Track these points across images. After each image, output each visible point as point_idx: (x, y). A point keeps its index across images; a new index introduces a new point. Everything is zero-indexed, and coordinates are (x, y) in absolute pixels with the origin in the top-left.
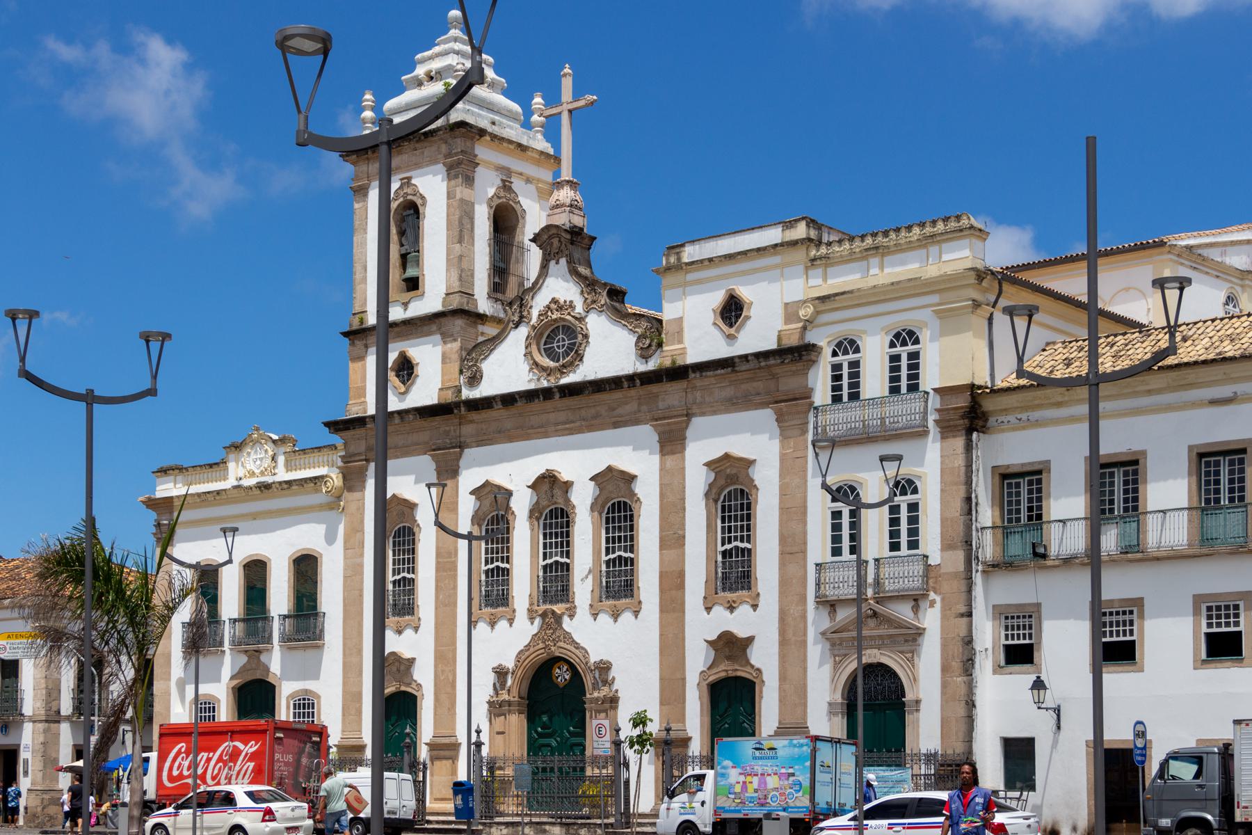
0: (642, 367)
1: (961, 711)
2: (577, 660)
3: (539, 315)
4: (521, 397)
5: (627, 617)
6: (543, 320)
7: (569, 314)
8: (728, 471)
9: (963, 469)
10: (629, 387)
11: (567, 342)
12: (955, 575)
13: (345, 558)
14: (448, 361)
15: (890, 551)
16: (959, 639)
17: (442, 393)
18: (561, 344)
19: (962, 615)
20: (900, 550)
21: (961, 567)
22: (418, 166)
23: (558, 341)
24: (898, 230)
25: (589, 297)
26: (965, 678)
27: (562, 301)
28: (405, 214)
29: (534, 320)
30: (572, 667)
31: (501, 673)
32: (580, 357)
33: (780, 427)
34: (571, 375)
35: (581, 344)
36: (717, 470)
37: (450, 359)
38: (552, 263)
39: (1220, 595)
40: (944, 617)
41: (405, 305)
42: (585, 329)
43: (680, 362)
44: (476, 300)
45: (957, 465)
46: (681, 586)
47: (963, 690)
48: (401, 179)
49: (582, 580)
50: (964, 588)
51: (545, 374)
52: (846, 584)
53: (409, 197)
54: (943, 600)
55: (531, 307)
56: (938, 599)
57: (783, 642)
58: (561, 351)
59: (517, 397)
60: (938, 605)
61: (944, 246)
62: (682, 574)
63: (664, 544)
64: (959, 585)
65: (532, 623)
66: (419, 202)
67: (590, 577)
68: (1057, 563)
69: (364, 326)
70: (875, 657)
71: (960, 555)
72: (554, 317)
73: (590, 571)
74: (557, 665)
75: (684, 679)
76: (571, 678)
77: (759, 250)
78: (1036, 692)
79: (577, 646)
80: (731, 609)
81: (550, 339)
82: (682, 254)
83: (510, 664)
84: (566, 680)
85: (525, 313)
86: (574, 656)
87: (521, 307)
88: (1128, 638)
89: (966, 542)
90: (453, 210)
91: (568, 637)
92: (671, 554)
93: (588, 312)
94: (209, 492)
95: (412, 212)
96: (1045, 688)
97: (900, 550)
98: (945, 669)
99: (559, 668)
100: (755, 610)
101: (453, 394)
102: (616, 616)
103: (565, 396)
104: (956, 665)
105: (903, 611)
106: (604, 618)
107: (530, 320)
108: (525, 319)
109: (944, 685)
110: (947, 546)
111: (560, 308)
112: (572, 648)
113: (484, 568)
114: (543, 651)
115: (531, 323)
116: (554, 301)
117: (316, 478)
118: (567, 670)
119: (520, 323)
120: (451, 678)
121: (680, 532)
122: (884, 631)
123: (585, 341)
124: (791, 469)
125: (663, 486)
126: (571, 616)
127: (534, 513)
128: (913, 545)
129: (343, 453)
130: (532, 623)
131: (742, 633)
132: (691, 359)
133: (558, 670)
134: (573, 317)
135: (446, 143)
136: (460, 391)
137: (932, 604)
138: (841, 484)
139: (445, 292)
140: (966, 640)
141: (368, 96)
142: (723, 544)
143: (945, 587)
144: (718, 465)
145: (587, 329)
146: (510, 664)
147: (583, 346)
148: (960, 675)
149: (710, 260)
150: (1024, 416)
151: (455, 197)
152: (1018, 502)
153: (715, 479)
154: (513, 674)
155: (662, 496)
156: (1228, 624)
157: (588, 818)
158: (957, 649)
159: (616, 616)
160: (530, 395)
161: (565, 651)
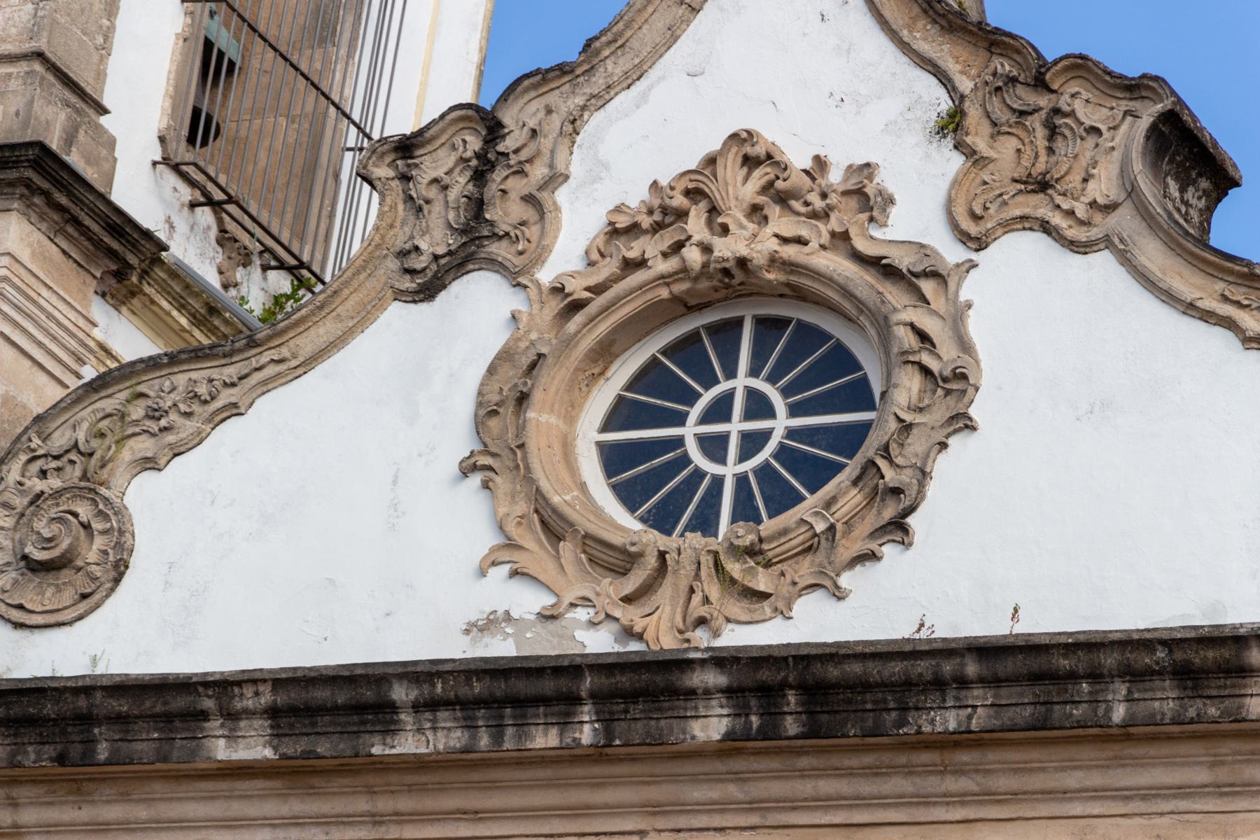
3: (614, 232)
6: (631, 265)
11: (781, 423)
18: (736, 427)
27: (799, 159)
35: (906, 428)
42: (948, 346)
44: (111, 143)
51: (611, 589)
55: (556, 179)
58: (730, 470)
59: (400, 693)
72: (726, 248)
85: (505, 213)
87: (480, 177)
93: (980, 243)
107: (540, 258)
108: (499, 250)
115: (546, 275)
119: (469, 258)
123: (938, 414)
145: (966, 346)
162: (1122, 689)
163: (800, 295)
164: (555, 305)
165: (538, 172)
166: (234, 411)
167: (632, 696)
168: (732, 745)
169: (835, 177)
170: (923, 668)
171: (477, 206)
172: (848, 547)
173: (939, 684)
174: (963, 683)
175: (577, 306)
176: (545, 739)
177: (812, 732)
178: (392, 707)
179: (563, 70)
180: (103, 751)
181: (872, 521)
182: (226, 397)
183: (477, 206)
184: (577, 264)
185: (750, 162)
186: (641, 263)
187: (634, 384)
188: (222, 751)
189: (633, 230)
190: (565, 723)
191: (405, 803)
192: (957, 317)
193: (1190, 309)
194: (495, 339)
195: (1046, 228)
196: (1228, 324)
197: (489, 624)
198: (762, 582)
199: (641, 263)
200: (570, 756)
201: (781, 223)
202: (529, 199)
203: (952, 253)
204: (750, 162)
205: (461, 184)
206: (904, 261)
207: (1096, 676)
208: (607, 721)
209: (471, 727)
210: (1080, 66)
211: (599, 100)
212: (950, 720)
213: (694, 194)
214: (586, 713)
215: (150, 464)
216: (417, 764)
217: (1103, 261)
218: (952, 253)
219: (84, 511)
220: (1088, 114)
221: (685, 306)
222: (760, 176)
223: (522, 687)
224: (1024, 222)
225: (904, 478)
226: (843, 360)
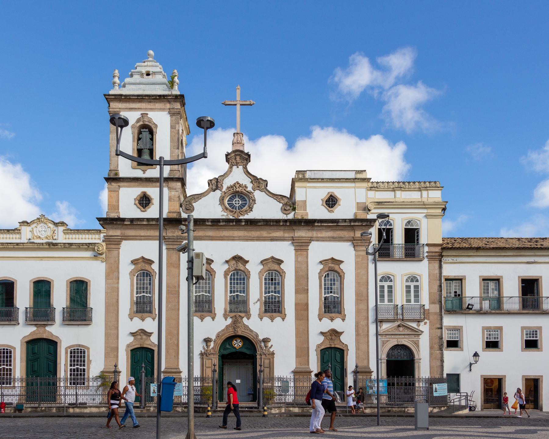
0: (284, 217)
1: (439, 363)
2: (252, 337)
4: (223, 221)
5: (278, 320)
7: (245, 190)
8: (330, 265)
9: (438, 275)
10: (283, 225)
11: (240, 202)
12: (435, 313)
13: (106, 283)
14: (172, 200)
15: (414, 302)
16: (438, 337)
17: (170, 214)
18: (237, 202)
19: (439, 328)
20: (411, 303)
21: (438, 311)
22: (152, 109)
23: (236, 201)
24: (414, 183)
25: (256, 184)
26: (440, 352)
27: (241, 183)
28: (142, 130)
29: (224, 189)
30: (243, 338)
31: (207, 341)
32: (251, 209)
33: (355, 250)
34: (246, 215)
36: (325, 264)
37: (174, 199)
38: (235, 167)
39: (531, 327)
40: (430, 329)
41: (144, 171)
43: (305, 218)
45: (435, 273)
46: (307, 309)
47: (439, 356)
48: (142, 114)
49: (254, 303)
50: (439, 318)
52: (390, 314)
53: (147, 123)
54: (430, 322)
56: (428, 321)
57: (358, 334)
60: (428, 324)
61: (430, 192)
62: (307, 305)
63: (297, 292)
64: (438, 317)
65: (226, 320)
66: (153, 126)
67: (259, 302)
68: (474, 312)
69: (117, 177)
70: (402, 342)
71: (437, 306)
73: (258, 300)
74: (235, 339)
75: (308, 348)
76: (244, 345)
77: (347, 179)
78: (475, 357)
79: (251, 331)
80: (332, 320)
81: (231, 200)
82: (306, 175)
83: (213, 337)
84: (240, 346)
85: (219, 186)
86: (250, 336)
88: (496, 340)
89: (440, 302)
90: (174, 134)
91: (246, 327)
92: (302, 296)
93: (255, 191)
94: (10, 243)
95: (147, 130)
96: (479, 356)
97: (411, 303)
98: (431, 348)
99: (236, 340)
100: (343, 321)
101: (177, 215)
102: (272, 319)
103: (247, 224)
104: (436, 346)
105: (414, 325)
106: (266, 320)
109: (431, 354)
110: (432, 302)
111: (240, 186)
112: (250, 333)
113: (194, 294)
114: (233, 332)
115: (223, 190)
116: (238, 183)
117: (89, 244)
118: (240, 341)
120: (176, 343)
121: (306, 288)
122: (407, 332)
124: (361, 268)
125: (296, 268)
126: (248, 319)
127: (226, 274)
128: (417, 301)
129: (105, 234)
130: (226, 320)
131: (339, 330)
132: (311, 217)
133: (235, 341)
134: (247, 192)
135: (170, 103)
136: (180, 214)
137: (425, 323)
138: (384, 275)
139: (169, 170)
140: (440, 337)
141: (117, 71)
142: (325, 294)
143: (431, 317)
144: (326, 262)
145: (255, 198)
146: (213, 337)
147: (252, 205)
148: (438, 350)
149: (323, 179)
150: (455, 259)
151: (176, 128)
152: (450, 289)
153: (323, 268)
154: (215, 342)
155: (296, 272)
156: (533, 337)
157: (200, 404)
158: (437, 340)
159: (272, 319)
160: (228, 221)
161: (245, 333)
162: (272, 223)
163: (241, 193)
164: (224, 193)
165: (221, 183)
166: (201, 199)
167: (238, 221)
168: (245, 225)
169: (243, 185)
170: (258, 220)
171: (217, 185)
172: (248, 211)
173: (259, 222)
174: (261, 221)
175: (226, 193)
176: (231, 224)
177: (250, 224)
178: (220, 221)
179: (222, 175)
180: (198, 223)
181: (249, 210)
182: (199, 198)
183: (217, 185)
184: (225, 190)
185: (238, 184)
186: (230, 190)
187: (229, 198)
188: (207, 224)
189: (229, 188)
190: (233, 223)
191: (220, 228)
192: (254, 196)
193: (270, 196)
194: (220, 195)
195: (259, 190)
196: (273, 198)
197: (223, 215)
198: (242, 213)
199: (230, 190)
200: (233, 225)
201: (240, 188)
202: (221, 185)
203: (253, 191)
204: (238, 184)
205: (215, 183)
206: (249, 192)
207: (270, 222)
208: (236, 223)
209: (226, 223)
210: (261, 179)
211: (225, 178)
212: (260, 224)
213: (234, 186)
214: (234, 222)
215: (195, 202)
216: (221, 225)
217: (264, 192)
218: (253, 191)
219: (190, 205)
220: (262, 182)
221: (233, 193)
222: (239, 185)
223: (230, 220)
224: (258, 189)
225: (252, 207)
226: (244, 198)
